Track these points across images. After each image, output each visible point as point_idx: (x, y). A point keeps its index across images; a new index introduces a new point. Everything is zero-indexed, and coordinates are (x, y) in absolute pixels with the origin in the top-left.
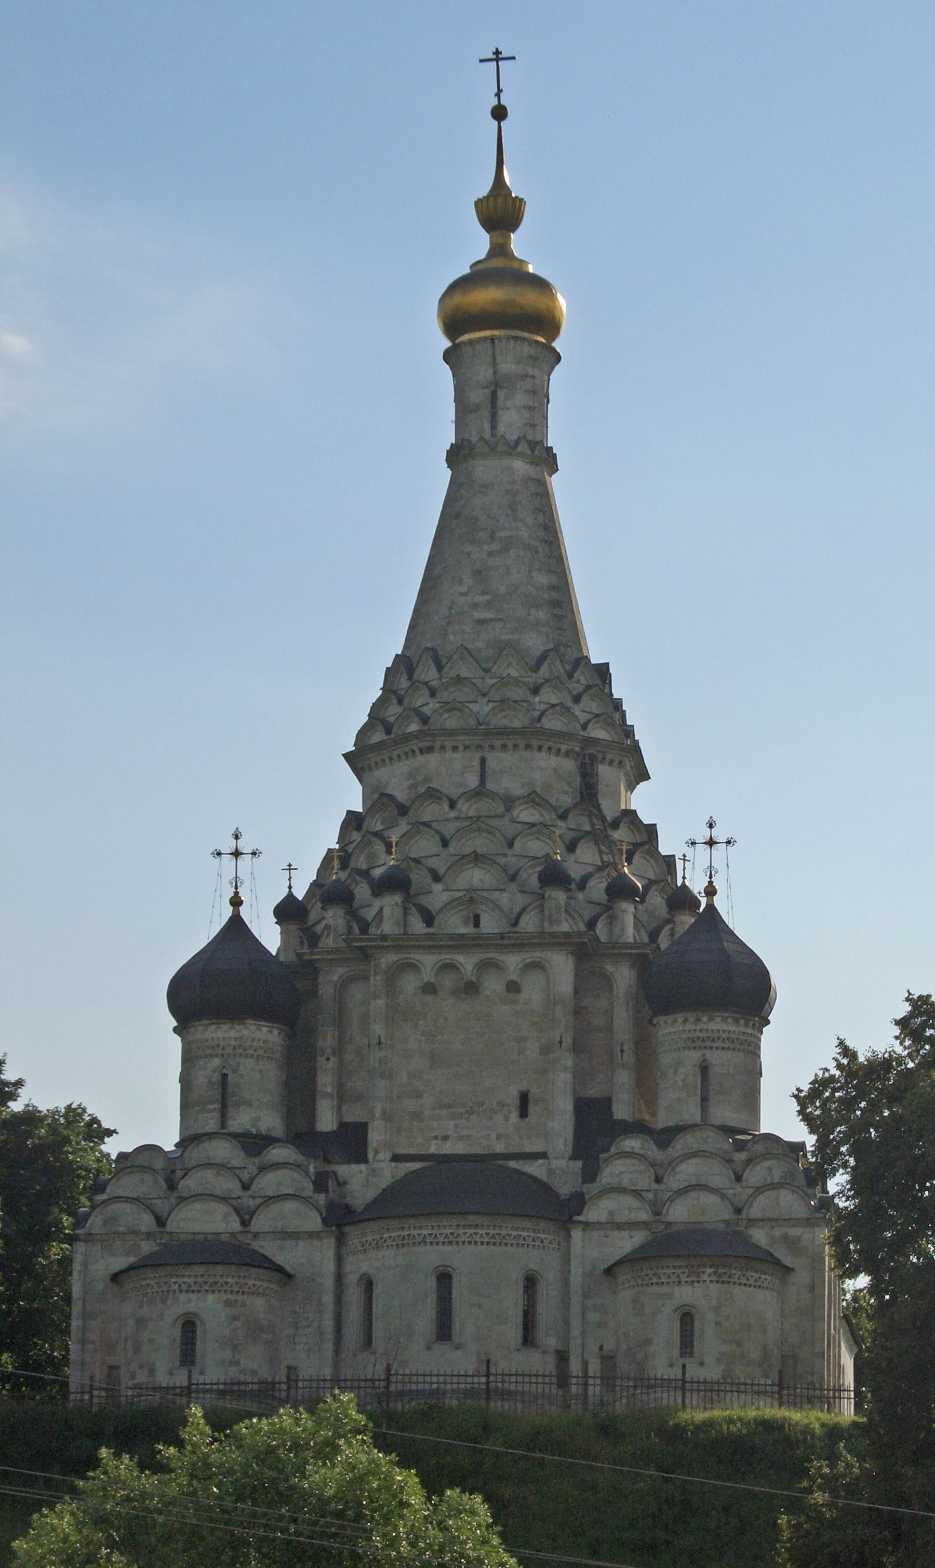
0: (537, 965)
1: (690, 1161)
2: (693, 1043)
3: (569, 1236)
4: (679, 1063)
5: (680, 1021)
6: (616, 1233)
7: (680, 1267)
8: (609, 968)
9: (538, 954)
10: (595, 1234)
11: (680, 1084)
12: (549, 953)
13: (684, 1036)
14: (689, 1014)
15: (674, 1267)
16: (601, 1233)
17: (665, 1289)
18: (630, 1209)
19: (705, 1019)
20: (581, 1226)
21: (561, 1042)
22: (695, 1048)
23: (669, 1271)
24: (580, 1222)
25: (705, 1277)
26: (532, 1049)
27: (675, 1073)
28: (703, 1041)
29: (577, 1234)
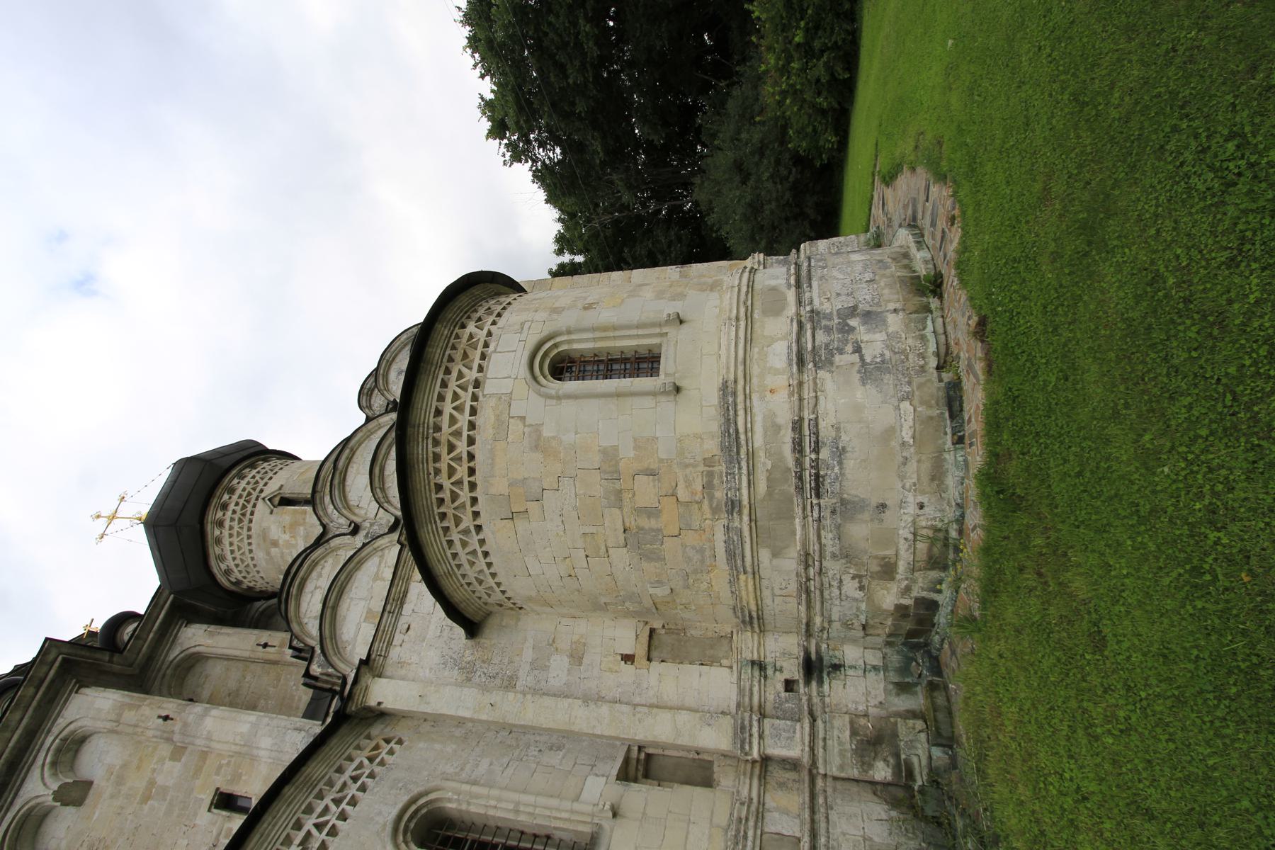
0: (74, 744)
1: (349, 481)
2: (246, 516)
3: (379, 715)
4: (264, 534)
5: (217, 532)
6: (407, 608)
7: (444, 385)
8: (175, 653)
9: (50, 741)
10: (395, 653)
11: (287, 537)
12: (60, 720)
13: (235, 524)
14: (210, 517)
15: (441, 398)
16: (398, 638)
17: (486, 419)
18: (377, 577)
19: (226, 497)
20: (367, 679)
21: (166, 718)
22: (252, 513)
23: (448, 408)
24: (356, 681)
25: (481, 335)
26: (170, 773)
27: (275, 544)
28: (248, 502)
29: (381, 693)
